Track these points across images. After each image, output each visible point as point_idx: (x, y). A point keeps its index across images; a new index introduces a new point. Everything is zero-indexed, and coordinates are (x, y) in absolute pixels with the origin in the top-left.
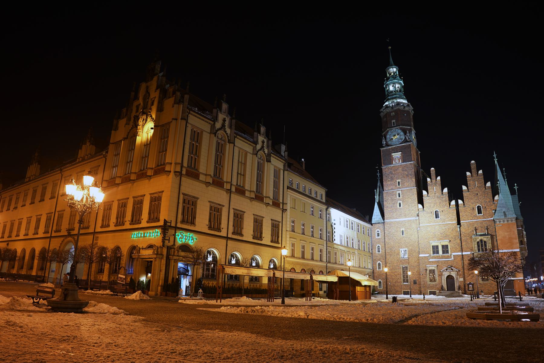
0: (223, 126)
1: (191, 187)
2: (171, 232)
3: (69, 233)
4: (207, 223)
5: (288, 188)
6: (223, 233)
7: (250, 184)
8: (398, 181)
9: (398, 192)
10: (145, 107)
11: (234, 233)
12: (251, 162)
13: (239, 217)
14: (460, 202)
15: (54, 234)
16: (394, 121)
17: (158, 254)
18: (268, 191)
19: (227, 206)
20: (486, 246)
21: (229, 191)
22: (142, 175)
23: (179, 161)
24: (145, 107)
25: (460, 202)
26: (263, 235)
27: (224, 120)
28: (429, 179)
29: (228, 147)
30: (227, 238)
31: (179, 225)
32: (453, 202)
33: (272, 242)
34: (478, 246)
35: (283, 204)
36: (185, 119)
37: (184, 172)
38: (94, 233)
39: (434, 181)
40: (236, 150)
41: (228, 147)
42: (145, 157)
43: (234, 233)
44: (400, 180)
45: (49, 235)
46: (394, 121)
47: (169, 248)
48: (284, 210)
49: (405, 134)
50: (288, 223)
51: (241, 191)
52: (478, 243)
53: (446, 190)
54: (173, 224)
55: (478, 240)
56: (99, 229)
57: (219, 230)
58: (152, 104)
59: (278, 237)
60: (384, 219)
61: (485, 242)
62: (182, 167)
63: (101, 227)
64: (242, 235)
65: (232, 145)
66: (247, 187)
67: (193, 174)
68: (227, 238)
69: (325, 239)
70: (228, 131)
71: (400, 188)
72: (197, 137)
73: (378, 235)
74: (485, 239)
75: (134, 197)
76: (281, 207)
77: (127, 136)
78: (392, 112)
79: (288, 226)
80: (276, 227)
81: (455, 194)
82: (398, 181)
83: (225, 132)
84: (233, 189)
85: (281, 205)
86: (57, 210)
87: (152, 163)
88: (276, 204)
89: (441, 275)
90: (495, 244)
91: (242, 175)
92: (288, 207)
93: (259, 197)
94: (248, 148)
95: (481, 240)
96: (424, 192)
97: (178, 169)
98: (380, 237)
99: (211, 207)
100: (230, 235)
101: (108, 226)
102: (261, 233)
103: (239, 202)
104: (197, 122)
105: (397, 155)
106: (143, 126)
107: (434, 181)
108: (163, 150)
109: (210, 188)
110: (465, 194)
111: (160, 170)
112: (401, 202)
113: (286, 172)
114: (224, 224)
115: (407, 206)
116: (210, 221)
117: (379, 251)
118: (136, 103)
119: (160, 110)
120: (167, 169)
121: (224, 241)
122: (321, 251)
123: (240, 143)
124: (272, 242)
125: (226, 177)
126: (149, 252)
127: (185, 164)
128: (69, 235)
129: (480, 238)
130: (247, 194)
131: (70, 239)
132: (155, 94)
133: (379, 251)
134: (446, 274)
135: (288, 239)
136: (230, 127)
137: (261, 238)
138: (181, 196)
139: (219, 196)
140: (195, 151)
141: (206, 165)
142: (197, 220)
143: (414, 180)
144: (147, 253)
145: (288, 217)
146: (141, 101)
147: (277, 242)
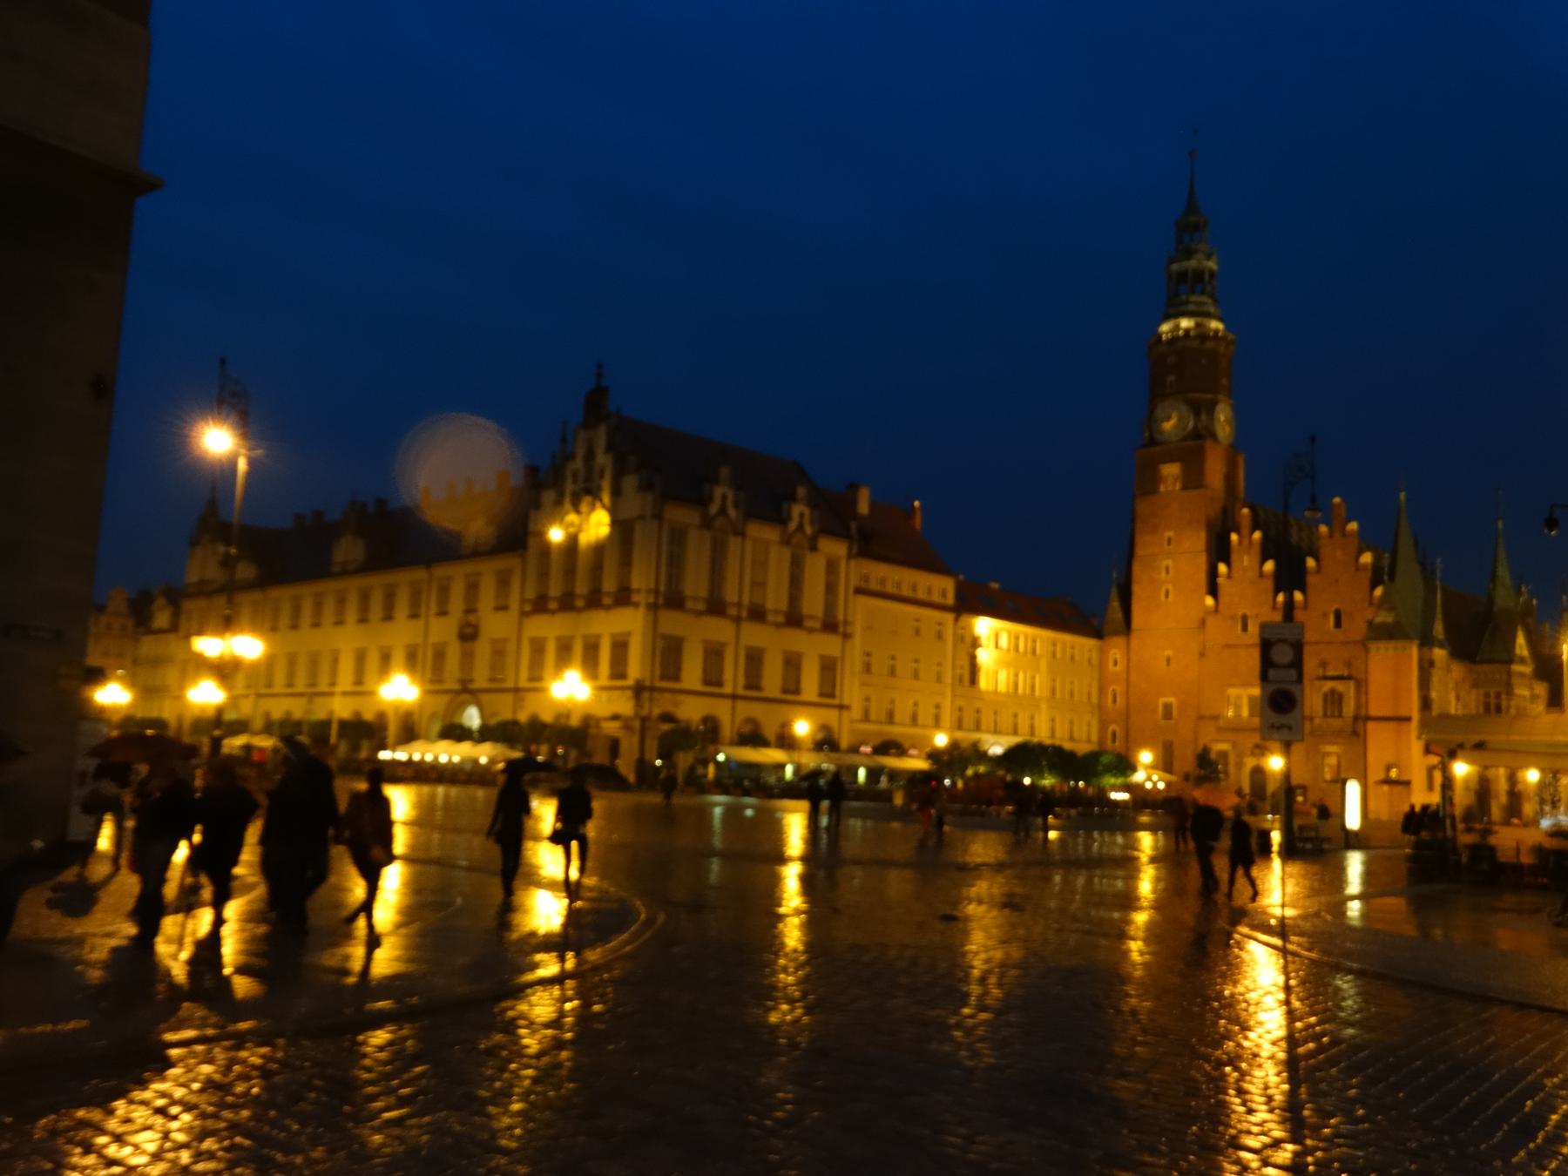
0: (723, 511)
1: (673, 623)
2: (646, 695)
5: (859, 591)
6: (728, 689)
7: (776, 599)
10: (589, 478)
12: (778, 561)
13: (755, 660)
14: (1298, 596)
17: (627, 727)
18: (813, 603)
20: (1340, 703)
21: (737, 620)
22: (595, 601)
23: (652, 586)
24: (589, 478)
25: (1298, 596)
27: (724, 498)
28: (1234, 537)
29: (734, 544)
30: (734, 697)
31: (658, 684)
32: (1281, 598)
33: (821, 695)
36: (658, 516)
37: (661, 601)
39: (1246, 542)
40: (749, 545)
41: (734, 544)
42: (597, 568)
47: (644, 720)
48: (847, 636)
49: (1197, 414)
51: (758, 614)
53: (1269, 566)
54: (648, 683)
56: (523, 683)
57: (720, 684)
58: (602, 476)
62: (656, 592)
65: (739, 540)
66: (770, 605)
68: (734, 697)
69: (949, 680)
70: (732, 513)
72: (678, 537)
73: (1116, 663)
76: (841, 629)
80: (829, 668)
81: (1290, 577)
84: (744, 613)
87: (609, 585)
88: (830, 626)
89: (1240, 765)
90: (1363, 700)
91: (759, 585)
92: (857, 630)
93: (794, 620)
94: (770, 534)
95: (1333, 691)
96: (1222, 568)
97: (651, 600)
98: (1118, 668)
100: (741, 691)
103: (754, 635)
104: (678, 514)
105: (1171, 470)
106: (589, 514)
107: (1246, 542)
108: (626, 562)
110: (1312, 580)
111: (623, 598)
112: (1170, 587)
113: (853, 563)
114: (728, 675)
117: (1115, 701)
119: (616, 493)
120: (635, 598)
121: (728, 703)
123: (756, 530)
125: (731, 594)
126: (616, 724)
127: (662, 588)
128: (465, 690)
129: (1329, 685)
130: (770, 617)
131: (465, 697)
132: (603, 459)
133: (1115, 701)
134: (1250, 762)
136: (736, 506)
137: (797, 691)
139: (719, 629)
140: (675, 563)
141: (695, 585)
143: (1203, 535)
144: (611, 728)
146: (578, 464)
147: (832, 696)
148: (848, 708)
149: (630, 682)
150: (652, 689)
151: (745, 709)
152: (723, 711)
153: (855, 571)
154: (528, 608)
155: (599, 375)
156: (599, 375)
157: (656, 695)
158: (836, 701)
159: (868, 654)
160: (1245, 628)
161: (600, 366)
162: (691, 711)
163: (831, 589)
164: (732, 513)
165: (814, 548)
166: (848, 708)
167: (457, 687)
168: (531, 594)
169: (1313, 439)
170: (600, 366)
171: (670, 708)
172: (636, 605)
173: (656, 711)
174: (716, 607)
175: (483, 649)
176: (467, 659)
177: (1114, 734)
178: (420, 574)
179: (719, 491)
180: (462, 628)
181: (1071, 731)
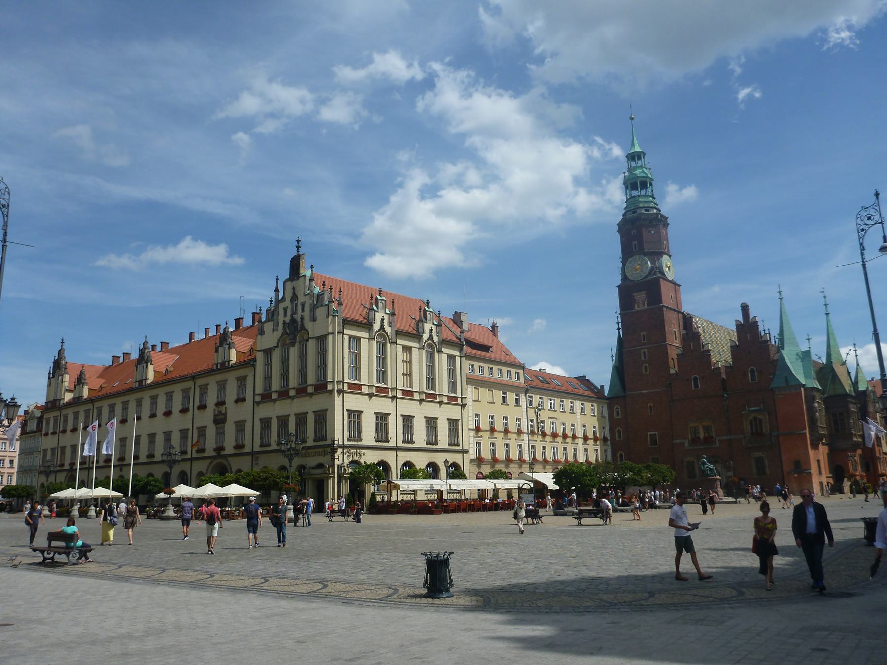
1: (353, 402)
2: (340, 451)
3: (219, 454)
4: (374, 434)
6: (392, 443)
7: (418, 384)
11: (403, 442)
12: (419, 357)
15: (195, 455)
18: (442, 386)
19: (393, 413)
20: (761, 426)
21: (394, 398)
26: (439, 438)
27: (383, 320)
30: (397, 449)
31: (346, 442)
33: (450, 445)
34: (752, 427)
35: (462, 398)
37: (346, 388)
38: (252, 454)
43: (403, 442)
45: (189, 456)
48: (463, 406)
50: (470, 419)
51: (408, 394)
52: (751, 421)
54: (341, 443)
55: (751, 418)
59: (458, 437)
60: (624, 390)
61: (760, 420)
63: (261, 446)
64: (413, 442)
65: (394, 346)
67: (355, 388)
68: (397, 449)
73: (618, 414)
74: (760, 417)
75: (296, 415)
76: (460, 402)
79: (471, 422)
83: (385, 331)
84: (399, 394)
85: (460, 399)
86: (195, 426)
88: (453, 400)
92: (469, 401)
95: (755, 418)
99: (377, 418)
100: (400, 444)
101: (269, 445)
102: (436, 436)
109: (373, 398)
116: (377, 433)
117: (620, 437)
118: (282, 306)
120: (330, 387)
122: (520, 446)
124: (450, 445)
130: (416, 396)
135: (471, 438)
138: (346, 414)
139: (384, 405)
142: (364, 435)
145: (470, 411)
146: (287, 303)
148: (467, 452)
149: (329, 442)
150: (344, 447)
151: (404, 457)
152: (390, 457)
153: (464, 367)
154: (258, 399)
155: (298, 247)
156: (298, 247)
157: (346, 450)
158: (461, 447)
159: (477, 416)
160: (696, 386)
161: (298, 241)
162: (370, 458)
163: (452, 373)
164: (388, 329)
165: (440, 351)
166: (467, 452)
167: (214, 454)
168: (259, 389)
169: (877, 194)
171: (355, 458)
173: (347, 461)
174: (382, 391)
175: (230, 428)
176: (220, 433)
177: (621, 455)
178: (190, 384)
179: (379, 316)
180: (215, 415)
181: (587, 455)
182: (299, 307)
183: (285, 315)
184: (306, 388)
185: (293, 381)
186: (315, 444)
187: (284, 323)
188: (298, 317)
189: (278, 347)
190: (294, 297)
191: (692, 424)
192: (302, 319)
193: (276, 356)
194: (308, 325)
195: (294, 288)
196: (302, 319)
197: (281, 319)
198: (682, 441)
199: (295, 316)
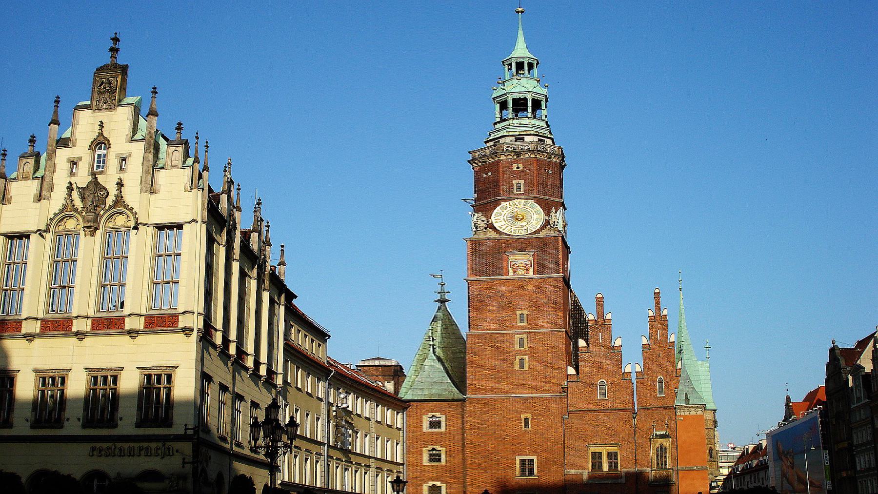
8: (519, 312)
9: (517, 337)
16: (522, 182)
44: (526, 312)
46: (522, 182)
71: (523, 327)
77: (48, 226)
78: (515, 162)
82: (519, 312)
115: (539, 368)
118: (63, 155)
146: (81, 149)
155: (114, 50)
156: (114, 50)
170: (116, 40)
172: (187, 331)
182: (112, 163)
183: (72, 173)
184: (122, 319)
185: (83, 303)
186: (141, 432)
187: (70, 188)
188: (108, 180)
189: (47, 231)
190: (100, 142)
191: (593, 449)
192: (120, 184)
193: (38, 252)
194: (133, 195)
195: (101, 125)
196: (120, 184)
197: (61, 179)
198: (580, 471)
199: (101, 179)
